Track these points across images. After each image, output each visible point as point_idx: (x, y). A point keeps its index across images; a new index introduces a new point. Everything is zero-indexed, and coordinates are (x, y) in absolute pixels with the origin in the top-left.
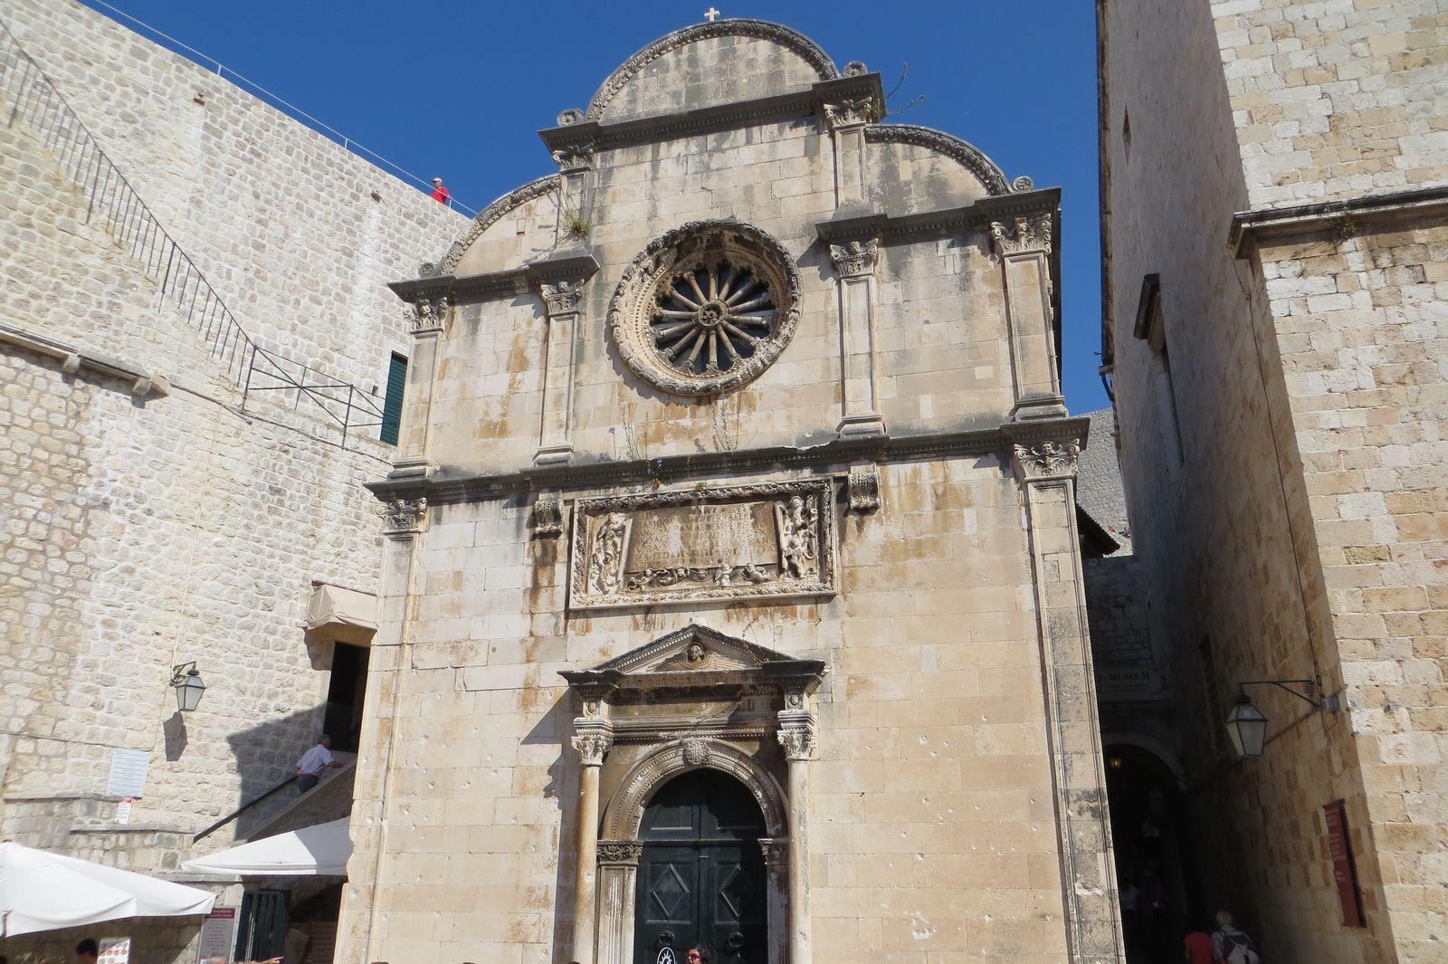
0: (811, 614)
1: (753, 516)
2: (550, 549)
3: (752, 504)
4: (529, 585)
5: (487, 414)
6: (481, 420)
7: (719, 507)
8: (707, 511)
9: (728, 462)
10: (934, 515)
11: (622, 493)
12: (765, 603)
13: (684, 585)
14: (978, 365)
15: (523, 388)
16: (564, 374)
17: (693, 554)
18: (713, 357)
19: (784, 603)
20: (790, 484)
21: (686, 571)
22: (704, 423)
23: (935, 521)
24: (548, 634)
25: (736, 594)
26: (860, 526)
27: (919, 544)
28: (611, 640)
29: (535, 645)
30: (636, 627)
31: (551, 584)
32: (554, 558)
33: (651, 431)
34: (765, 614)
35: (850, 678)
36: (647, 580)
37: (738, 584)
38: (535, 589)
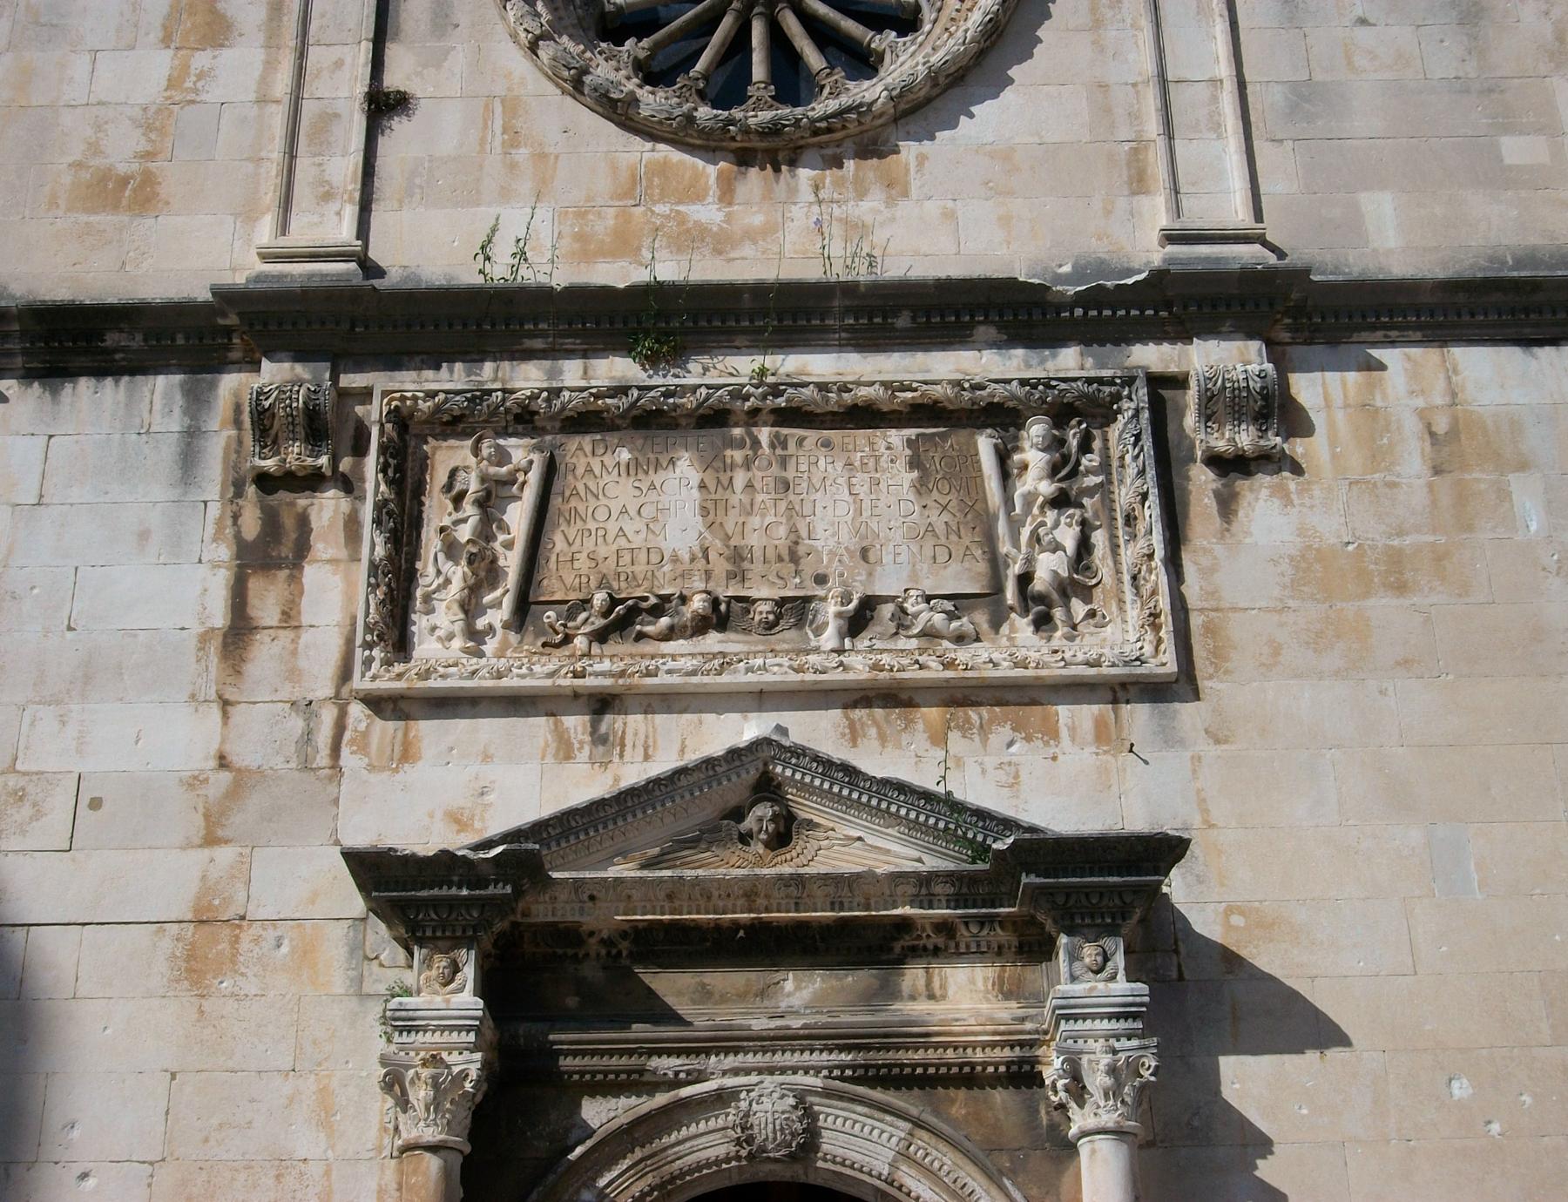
0: (1102, 734)
1: (914, 463)
2: (288, 522)
3: (912, 432)
4: (219, 617)
5: (95, 148)
6: (78, 165)
7: (812, 436)
8: (779, 442)
9: (847, 311)
10: (1430, 486)
11: (528, 378)
12: (963, 696)
13: (713, 641)
14: (1508, 129)
15: (213, 94)
16: (339, 64)
17: (738, 559)
18: (759, 71)
19: (1021, 696)
20: (1023, 382)
21: (715, 602)
22: (758, 220)
23: (1434, 503)
24: (278, 762)
25: (876, 667)
26: (1227, 504)
27: (1396, 559)
28: (482, 786)
29: (236, 791)
30: (565, 751)
31: (290, 618)
32: (302, 549)
33: (604, 224)
34: (965, 728)
35: (1229, 911)
36: (600, 622)
37: (879, 645)
38: (238, 632)
